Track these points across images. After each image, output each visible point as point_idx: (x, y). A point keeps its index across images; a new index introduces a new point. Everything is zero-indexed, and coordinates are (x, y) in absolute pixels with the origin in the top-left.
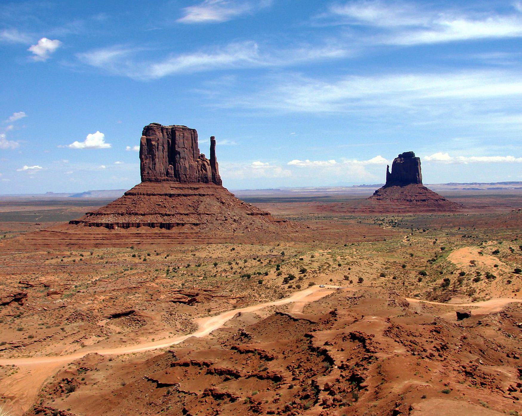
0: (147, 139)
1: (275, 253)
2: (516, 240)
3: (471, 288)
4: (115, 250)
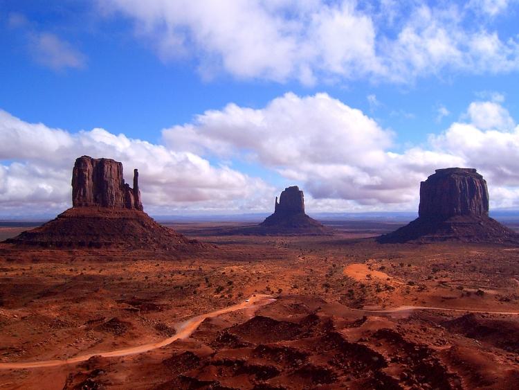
1: (193, 268)
3: (375, 297)
4: (52, 265)
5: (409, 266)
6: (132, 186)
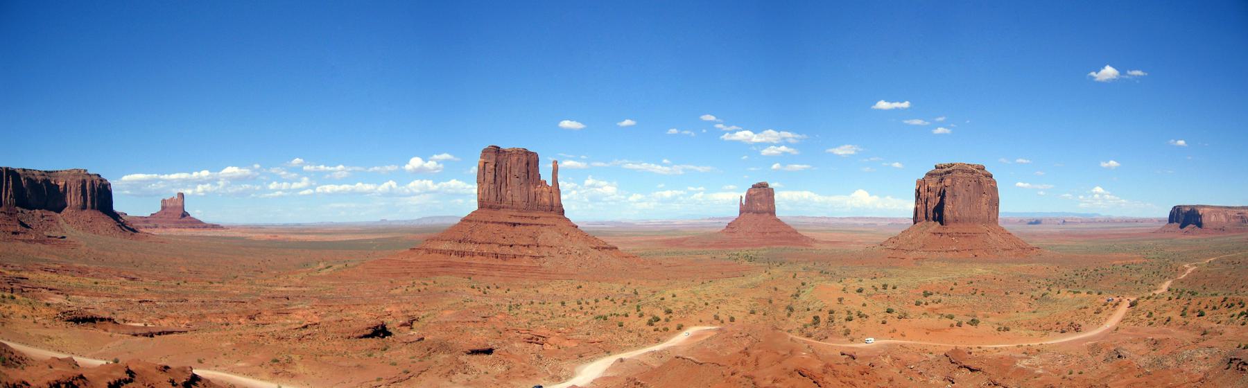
0: (485, 163)
2: (875, 278)
5: (894, 288)
6: (550, 183)
